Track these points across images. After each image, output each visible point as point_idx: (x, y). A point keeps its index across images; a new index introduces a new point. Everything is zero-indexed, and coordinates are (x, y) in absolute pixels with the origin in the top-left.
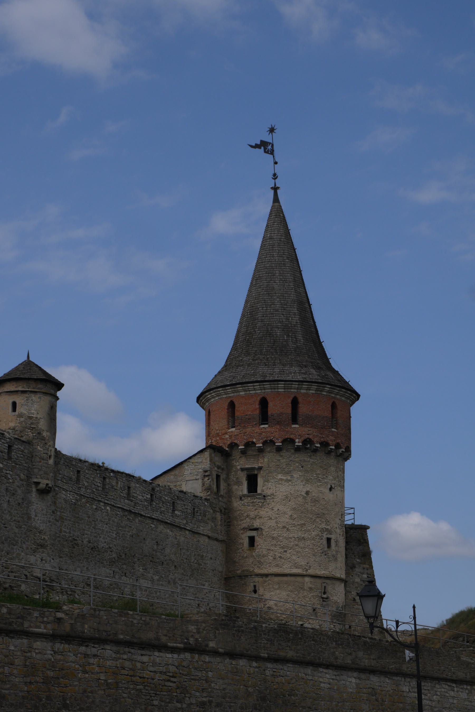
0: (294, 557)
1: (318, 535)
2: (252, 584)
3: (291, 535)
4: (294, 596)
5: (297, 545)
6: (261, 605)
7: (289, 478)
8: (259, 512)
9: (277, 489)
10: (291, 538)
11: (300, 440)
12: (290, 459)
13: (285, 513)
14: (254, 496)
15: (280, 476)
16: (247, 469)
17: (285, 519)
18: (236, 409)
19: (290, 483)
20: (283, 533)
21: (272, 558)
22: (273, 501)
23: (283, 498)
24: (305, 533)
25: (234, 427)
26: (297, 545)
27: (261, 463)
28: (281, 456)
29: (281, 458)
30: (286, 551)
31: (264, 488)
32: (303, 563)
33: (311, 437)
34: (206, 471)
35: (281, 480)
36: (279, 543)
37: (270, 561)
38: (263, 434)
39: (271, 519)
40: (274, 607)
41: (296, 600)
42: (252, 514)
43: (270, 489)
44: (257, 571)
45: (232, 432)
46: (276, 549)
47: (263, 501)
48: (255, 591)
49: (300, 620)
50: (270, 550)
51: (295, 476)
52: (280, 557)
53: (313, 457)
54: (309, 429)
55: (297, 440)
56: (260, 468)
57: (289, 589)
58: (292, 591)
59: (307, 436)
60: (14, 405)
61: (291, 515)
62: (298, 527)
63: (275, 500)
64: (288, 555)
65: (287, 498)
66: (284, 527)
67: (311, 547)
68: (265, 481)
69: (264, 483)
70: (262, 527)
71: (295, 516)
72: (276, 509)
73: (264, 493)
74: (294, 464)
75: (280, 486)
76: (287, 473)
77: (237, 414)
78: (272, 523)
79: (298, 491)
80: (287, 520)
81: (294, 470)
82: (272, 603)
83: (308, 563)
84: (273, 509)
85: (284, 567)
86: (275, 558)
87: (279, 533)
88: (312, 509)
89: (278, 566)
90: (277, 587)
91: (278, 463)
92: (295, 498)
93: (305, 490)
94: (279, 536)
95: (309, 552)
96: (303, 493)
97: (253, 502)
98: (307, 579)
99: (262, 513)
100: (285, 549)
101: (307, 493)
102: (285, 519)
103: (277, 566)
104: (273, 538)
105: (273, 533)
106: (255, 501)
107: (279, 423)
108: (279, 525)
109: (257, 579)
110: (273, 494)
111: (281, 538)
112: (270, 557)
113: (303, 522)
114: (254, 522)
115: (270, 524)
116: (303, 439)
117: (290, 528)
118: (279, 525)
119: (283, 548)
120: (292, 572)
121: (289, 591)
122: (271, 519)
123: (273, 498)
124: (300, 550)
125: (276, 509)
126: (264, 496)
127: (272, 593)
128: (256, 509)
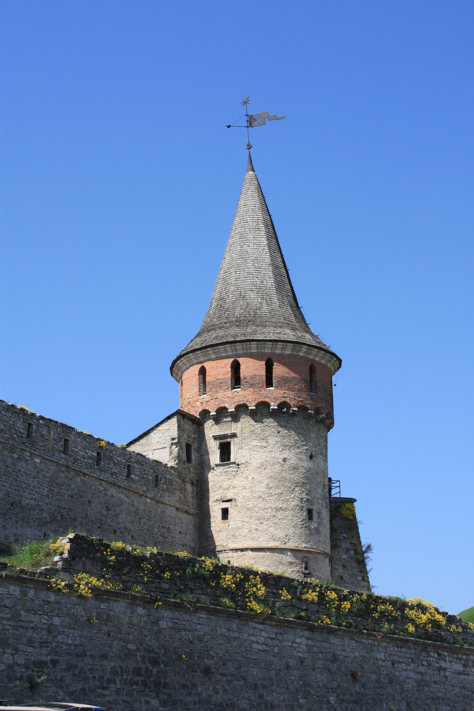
1: (298, 506)
3: (268, 506)
5: (274, 516)
7: (264, 444)
8: (232, 482)
10: (267, 509)
11: (276, 404)
13: (260, 482)
14: (227, 464)
19: (266, 449)
20: (259, 504)
21: (247, 531)
22: (247, 470)
23: (258, 465)
24: (283, 503)
26: (274, 516)
30: (261, 523)
32: (281, 535)
33: (287, 400)
34: (173, 439)
36: (255, 514)
37: (245, 534)
38: (236, 398)
39: (245, 488)
42: (225, 485)
46: (251, 520)
50: (245, 522)
52: (256, 529)
53: (290, 422)
54: (285, 392)
55: (272, 404)
57: (266, 564)
61: (268, 484)
62: (276, 496)
63: (249, 468)
65: (262, 466)
66: (260, 497)
67: (290, 518)
70: (236, 498)
71: (272, 485)
72: (250, 478)
74: (270, 430)
83: (286, 536)
85: (261, 540)
87: (255, 503)
88: (290, 478)
89: (254, 539)
93: (282, 457)
94: (255, 507)
95: (288, 523)
96: (280, 461)
99: (236, 482)
100: (262, 521)
101: (284, 460)
103: (253, 539)
104: (248, 509)
105: (248, 503)
107: (252, 385)
111: (257, 509)
112: (244, 530)
113: (280, 491)
115: (244, 494)
116: (278, 402)
118: (254, 495)
119: (259, 519)
121: (267, 566)
124: (277, 521)
125: (250, 478)
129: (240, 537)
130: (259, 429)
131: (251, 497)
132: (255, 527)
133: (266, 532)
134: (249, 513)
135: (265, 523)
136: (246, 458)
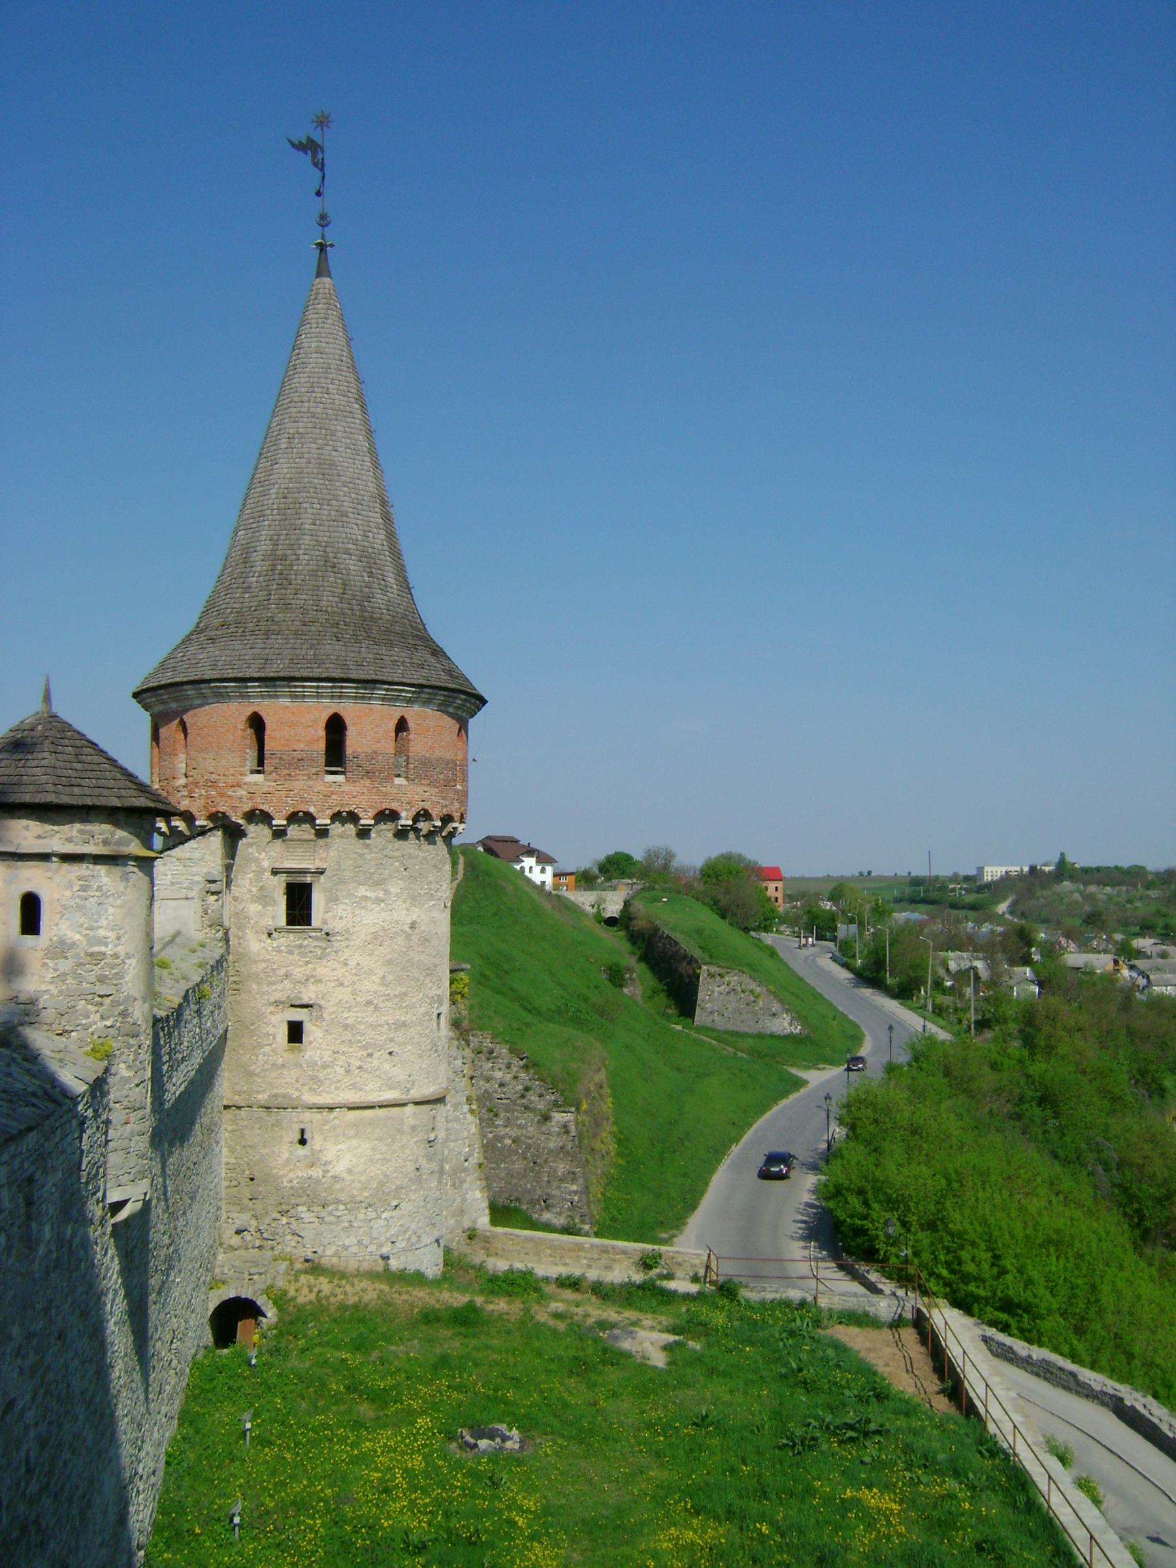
2: (296, 1129)
3: (383, 1019)
4: (384, 1148)
6: (316, 1173)
7: (381, 895)
8: (314, 969)
10: (381, 1025)
12: (385, 853)
13: (371, 972)
14: (303, 931)
15: (362, 891)
16: (289, 872)
17: (370, 985)
18: (267, 732)
21: (342, 1071)
22: (347, 946)
23: (368, 938)
25: (259, 772)
26: (391, 1040)
27: (321, 859)
30: (370, 1055)
31: (327, 916)
33: (427, 805)
35: (366, 898)
37: (339, 1078)
39: (342, 985)
40: (345, 1175)
41: (388, 1157)
42: (298, 972)
43: (341, 918)
44: (309, 1098)
45: (256, 784)
47: (324, 944)
48: (303, 1142)
49: (394, 1198)
51: (392, 890)
52: (360, 1067)
56: (321, 872)
58: (380, 1139)
60: (31, 913)
61: (384, 976)
63: (351, 943)
64: (376, 1063)
65: (376, 938)
66: (369, 1003)
68: (329, 901)
69: (327, 904)
70: (322, 1003)
71: (390, 977)
72: (352, 963)
73: (326, 928)
78: (343, 994)
79: (397, 922)
80: (376, 987)
81: (391, 876)
82: (340, 1168)
84: (346, 964)
85: (368, 1088)
86: (347, 1072)
89: (355, 1088)
90: (351, 1132)
91: (360, 862)
92: (392, 938)
97: (300, 946)
98: (410, 1109)
99: (322, 971)
102: (370, 985)
103: (353, 1086)
104: (346, 1027)
105: (345, 1015)
106: (306, 943)
109: (308, 1115)
110: (347, 931)
111: (362, 1027)
112: (338, 1069)
114: (303, 989)
115: (340, 997)
118: (358, 999)
119: (365, 1048)
120: (381, 1099)
123: (347, 939)
125: (352, 963)
126: (327, 934)
127: (342, 1146)
128: (308, 963)
129: (328, 1082)
130: (374, 863)
131: (353, 1003)
132: (358, 1063)
134: (348, 1035)
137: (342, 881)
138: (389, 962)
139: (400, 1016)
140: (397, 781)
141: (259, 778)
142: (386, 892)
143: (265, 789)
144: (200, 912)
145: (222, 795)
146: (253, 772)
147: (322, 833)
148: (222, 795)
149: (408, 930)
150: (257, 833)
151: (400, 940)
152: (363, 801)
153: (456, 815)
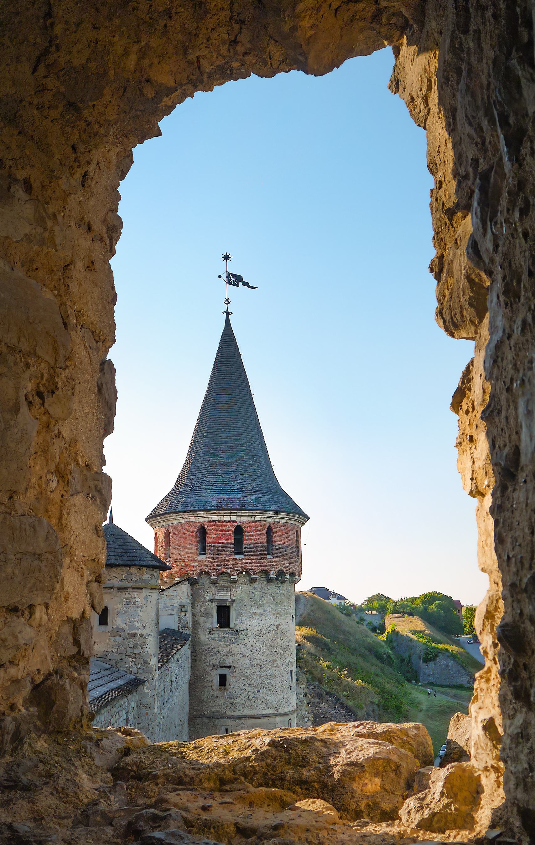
0: (267, 697)
3: (264, 674)
7: (262, 612)
9: (251, 624)
13: (258, 649)
15: (254, 610)
16: (218, 601)
21: (245, 699)
28: (255, 588)
29: (254, 591)
30: (259, 691)
33: (283, 568)
35: (255, 613)
36: (252, 682)
39: (245, 656)
42: (224, 650)
44: (229, 713)
46: (250, 689)
47: (236, 637)
56: (233, 601)
59: (280, 567)
64: (262, 695)
65: (260, 634)
66: (258, 665)
68: (237, 615)
70: (235, 665)
75: (254, 620)
76: (261, 606)
77: (208, 541)
78: (246, 661)
91: (251, 596)
92: (268, 633)
99: (235, 649)
104: (247, 677)
108: (252, 663)
109: (229, 722)
112: (243, 698)
117: (263, 666)
118: (252, 663)
122: (245, 656)
126: (237, 631)
128: (228, 646)
132: (253, 695)
133: (262, 700)
135: (262, 691)
136: (245, 625)
137: (244, 605)
138: (267, 645)
139: (272, 672)
140: (269, 557)
141: (203, 557)
142: (265, 610)
143: (207, 562)
144: (177, 621)
145: (187, 565)
146: (201, 554)
147: (234, 581)
148: (187, 565)
149: (276, 629)
150: (204, 580)
151: (272, 634)
152: (252, 566)
153: (297, 573)
